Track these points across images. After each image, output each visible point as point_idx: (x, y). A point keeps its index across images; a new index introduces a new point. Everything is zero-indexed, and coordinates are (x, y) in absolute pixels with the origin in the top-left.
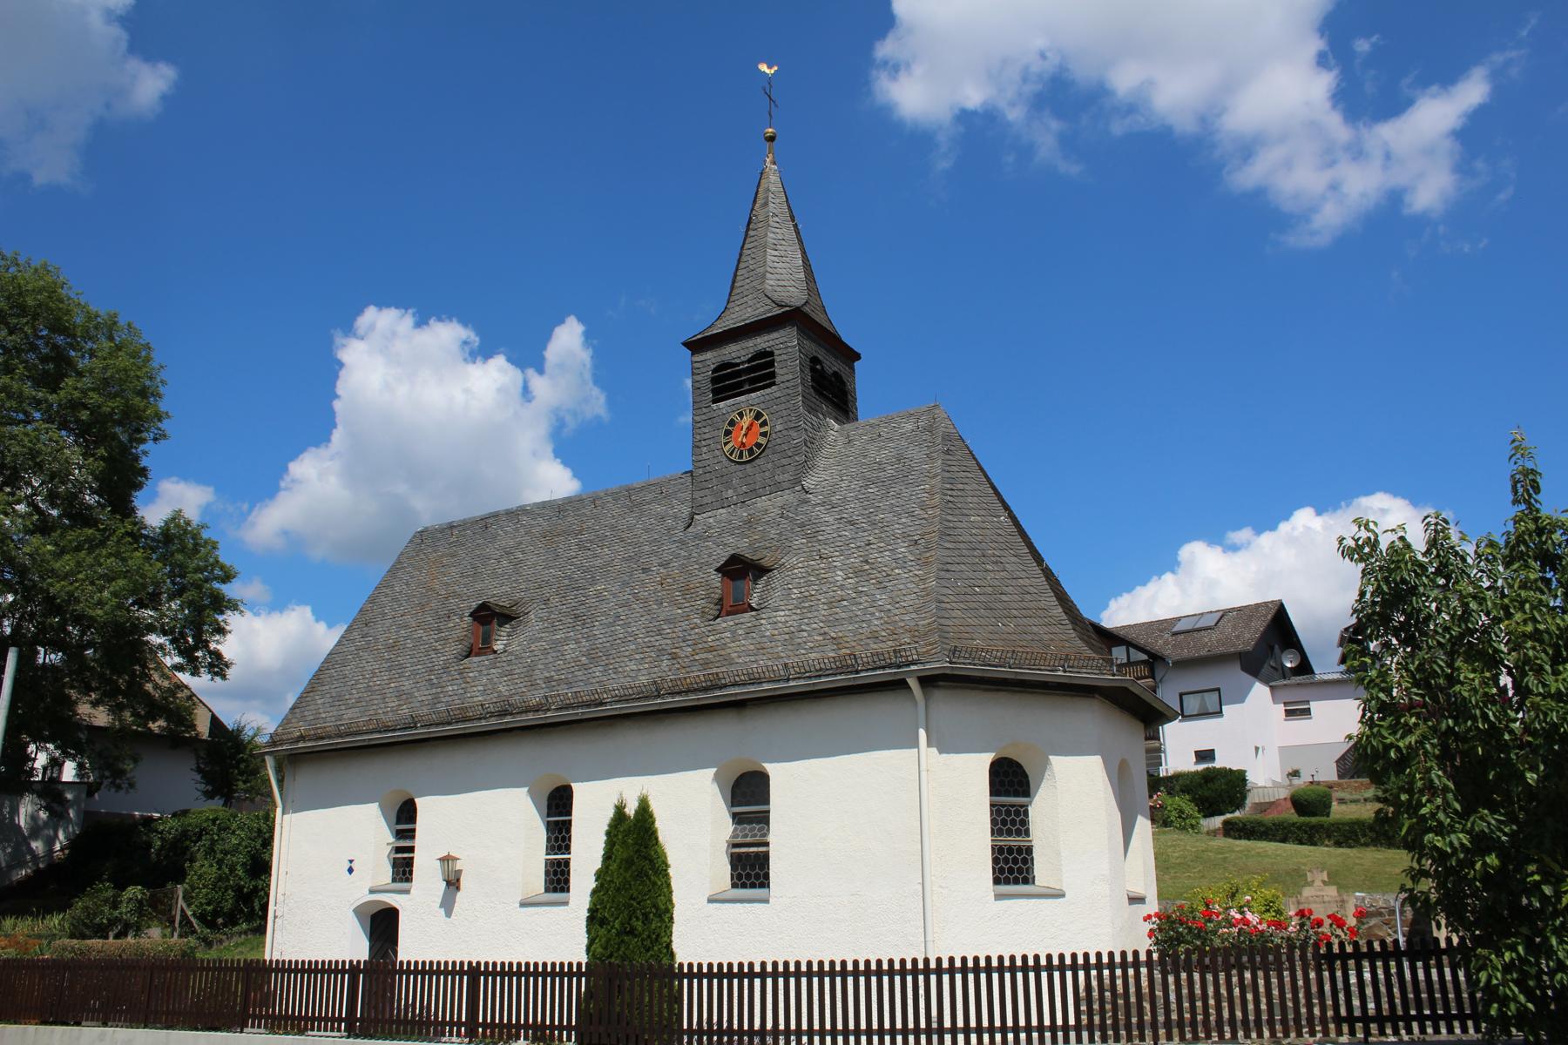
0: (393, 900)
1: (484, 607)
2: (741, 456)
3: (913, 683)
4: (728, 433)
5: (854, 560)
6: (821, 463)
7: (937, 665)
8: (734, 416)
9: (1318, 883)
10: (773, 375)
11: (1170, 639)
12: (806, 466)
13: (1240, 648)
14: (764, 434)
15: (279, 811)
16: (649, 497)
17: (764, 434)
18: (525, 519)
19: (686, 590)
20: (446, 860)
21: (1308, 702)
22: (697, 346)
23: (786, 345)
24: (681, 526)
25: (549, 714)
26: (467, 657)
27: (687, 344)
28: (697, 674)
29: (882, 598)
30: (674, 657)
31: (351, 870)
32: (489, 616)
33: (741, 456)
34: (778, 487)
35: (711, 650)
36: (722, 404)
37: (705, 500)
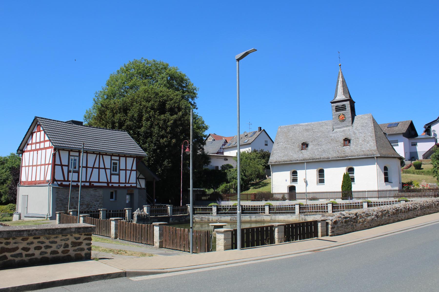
0: (294, 184)
1: (304, 143)
2: (341, 121)
3: (375, 157)
4: (339, 117)
8: (340, 114)
9: (424, 182)
10: (346, 109)
11: (387, 129)
13: (403, 132)
14: (345, 118)
15: (271, 173)
17: (345, 118)
20: (304, 179)
21: (417, 142)
23: (347, 104)
24: (331, 131)
25: (321, 160)
26: (302, 150)
27: (331, 102)
28: (343, 155)
30: (338, 152)
31: (286, 181)
33: (341, 121)
34: (347, 126)
35: (344, 151)
36: (337, 112)
37: (335, 127)
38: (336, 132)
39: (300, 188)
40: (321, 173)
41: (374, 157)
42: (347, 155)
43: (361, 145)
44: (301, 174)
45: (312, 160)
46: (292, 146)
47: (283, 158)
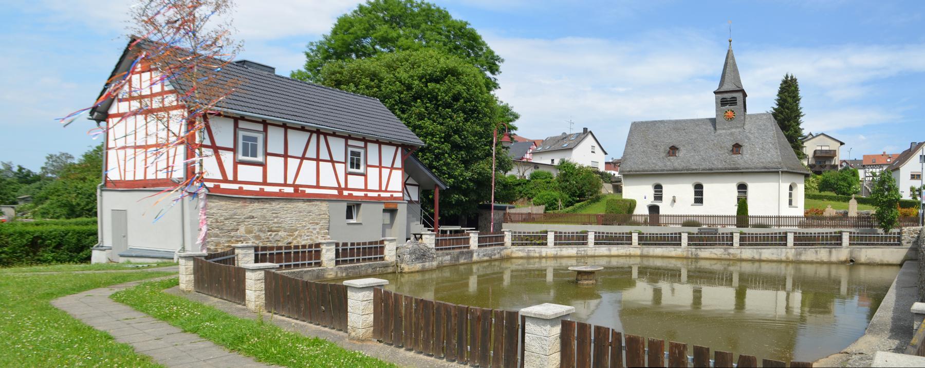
0: (657, 203)
3: (780, 172)
5: (761, 146)
6: (746, 123)
7: (786, 170)
12: (744, 124)
16: (700, 123)
18: (666, 124)
19: (721, 147)
20: (674, 197)
22: (715, 93)
28: (733, 166)
29: (769, 155)
32: (673, 150)
34: (737, 127)
38: (720, 135)
39: (665, 209)
40: (699, 189)
41: (778, 172)
42: (739, 166)
43: (758, 155)
44: (669, 189)
45: (686, 172)
46: (655, 151)
47: (641, 167)
